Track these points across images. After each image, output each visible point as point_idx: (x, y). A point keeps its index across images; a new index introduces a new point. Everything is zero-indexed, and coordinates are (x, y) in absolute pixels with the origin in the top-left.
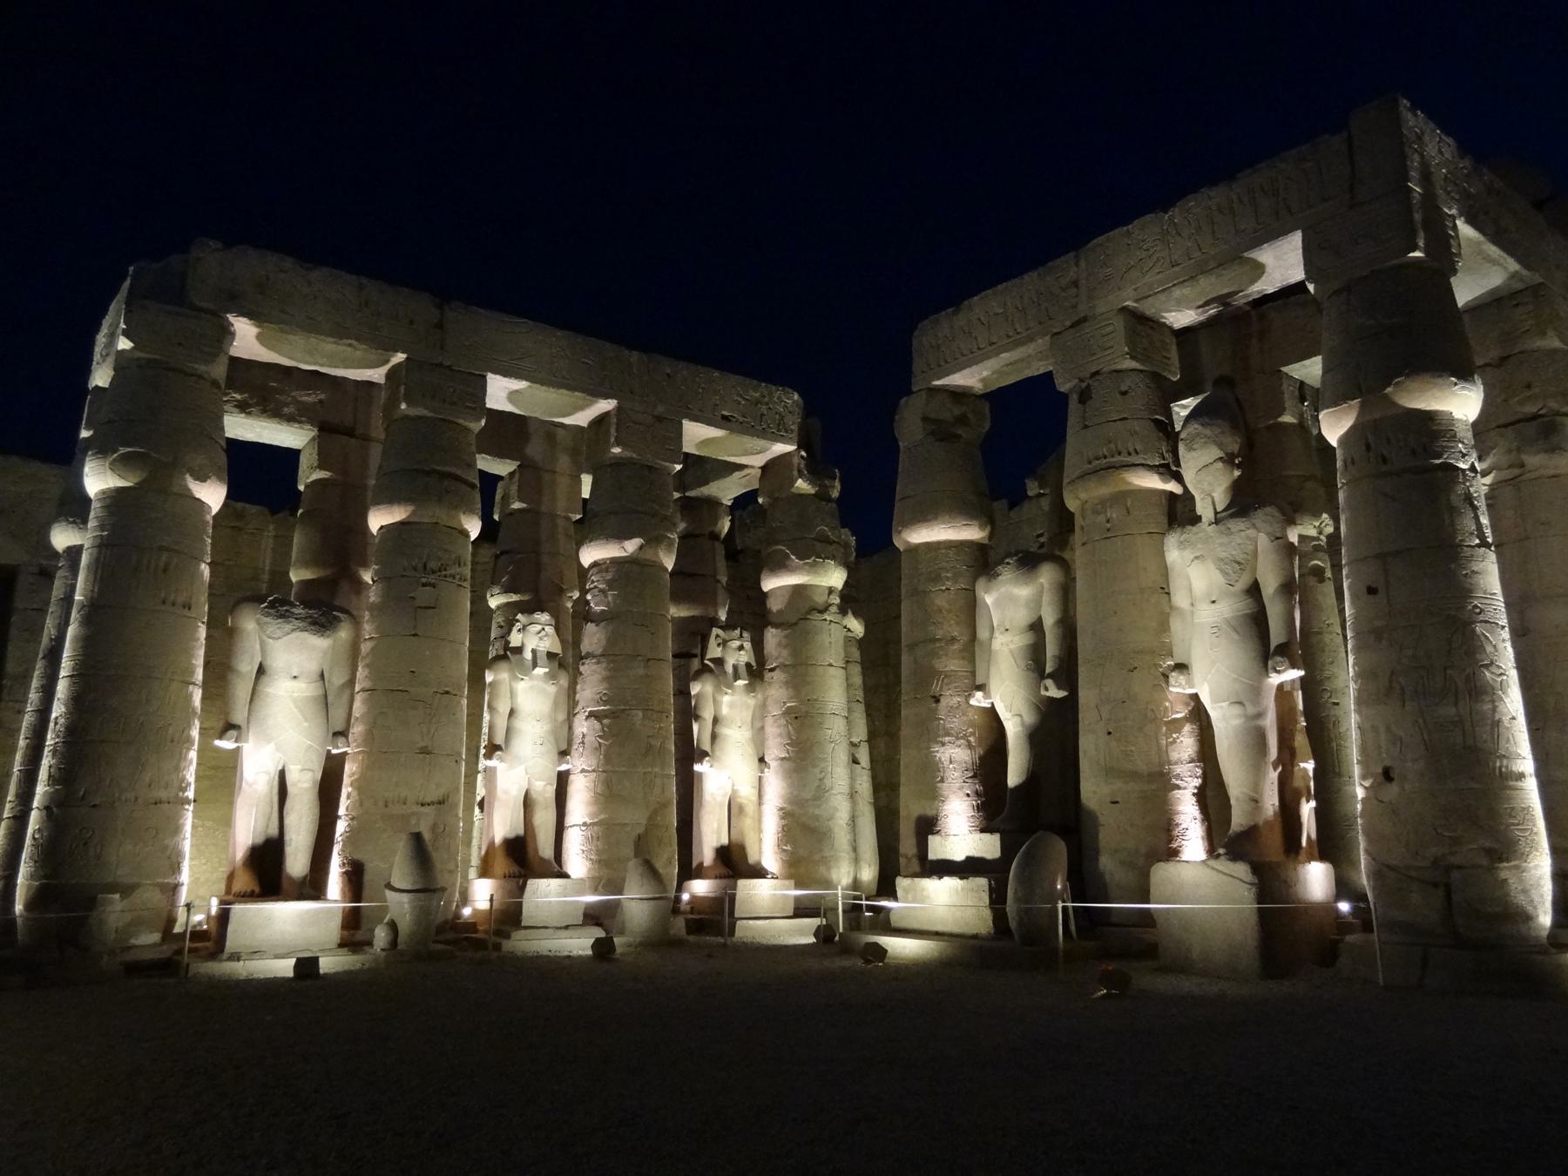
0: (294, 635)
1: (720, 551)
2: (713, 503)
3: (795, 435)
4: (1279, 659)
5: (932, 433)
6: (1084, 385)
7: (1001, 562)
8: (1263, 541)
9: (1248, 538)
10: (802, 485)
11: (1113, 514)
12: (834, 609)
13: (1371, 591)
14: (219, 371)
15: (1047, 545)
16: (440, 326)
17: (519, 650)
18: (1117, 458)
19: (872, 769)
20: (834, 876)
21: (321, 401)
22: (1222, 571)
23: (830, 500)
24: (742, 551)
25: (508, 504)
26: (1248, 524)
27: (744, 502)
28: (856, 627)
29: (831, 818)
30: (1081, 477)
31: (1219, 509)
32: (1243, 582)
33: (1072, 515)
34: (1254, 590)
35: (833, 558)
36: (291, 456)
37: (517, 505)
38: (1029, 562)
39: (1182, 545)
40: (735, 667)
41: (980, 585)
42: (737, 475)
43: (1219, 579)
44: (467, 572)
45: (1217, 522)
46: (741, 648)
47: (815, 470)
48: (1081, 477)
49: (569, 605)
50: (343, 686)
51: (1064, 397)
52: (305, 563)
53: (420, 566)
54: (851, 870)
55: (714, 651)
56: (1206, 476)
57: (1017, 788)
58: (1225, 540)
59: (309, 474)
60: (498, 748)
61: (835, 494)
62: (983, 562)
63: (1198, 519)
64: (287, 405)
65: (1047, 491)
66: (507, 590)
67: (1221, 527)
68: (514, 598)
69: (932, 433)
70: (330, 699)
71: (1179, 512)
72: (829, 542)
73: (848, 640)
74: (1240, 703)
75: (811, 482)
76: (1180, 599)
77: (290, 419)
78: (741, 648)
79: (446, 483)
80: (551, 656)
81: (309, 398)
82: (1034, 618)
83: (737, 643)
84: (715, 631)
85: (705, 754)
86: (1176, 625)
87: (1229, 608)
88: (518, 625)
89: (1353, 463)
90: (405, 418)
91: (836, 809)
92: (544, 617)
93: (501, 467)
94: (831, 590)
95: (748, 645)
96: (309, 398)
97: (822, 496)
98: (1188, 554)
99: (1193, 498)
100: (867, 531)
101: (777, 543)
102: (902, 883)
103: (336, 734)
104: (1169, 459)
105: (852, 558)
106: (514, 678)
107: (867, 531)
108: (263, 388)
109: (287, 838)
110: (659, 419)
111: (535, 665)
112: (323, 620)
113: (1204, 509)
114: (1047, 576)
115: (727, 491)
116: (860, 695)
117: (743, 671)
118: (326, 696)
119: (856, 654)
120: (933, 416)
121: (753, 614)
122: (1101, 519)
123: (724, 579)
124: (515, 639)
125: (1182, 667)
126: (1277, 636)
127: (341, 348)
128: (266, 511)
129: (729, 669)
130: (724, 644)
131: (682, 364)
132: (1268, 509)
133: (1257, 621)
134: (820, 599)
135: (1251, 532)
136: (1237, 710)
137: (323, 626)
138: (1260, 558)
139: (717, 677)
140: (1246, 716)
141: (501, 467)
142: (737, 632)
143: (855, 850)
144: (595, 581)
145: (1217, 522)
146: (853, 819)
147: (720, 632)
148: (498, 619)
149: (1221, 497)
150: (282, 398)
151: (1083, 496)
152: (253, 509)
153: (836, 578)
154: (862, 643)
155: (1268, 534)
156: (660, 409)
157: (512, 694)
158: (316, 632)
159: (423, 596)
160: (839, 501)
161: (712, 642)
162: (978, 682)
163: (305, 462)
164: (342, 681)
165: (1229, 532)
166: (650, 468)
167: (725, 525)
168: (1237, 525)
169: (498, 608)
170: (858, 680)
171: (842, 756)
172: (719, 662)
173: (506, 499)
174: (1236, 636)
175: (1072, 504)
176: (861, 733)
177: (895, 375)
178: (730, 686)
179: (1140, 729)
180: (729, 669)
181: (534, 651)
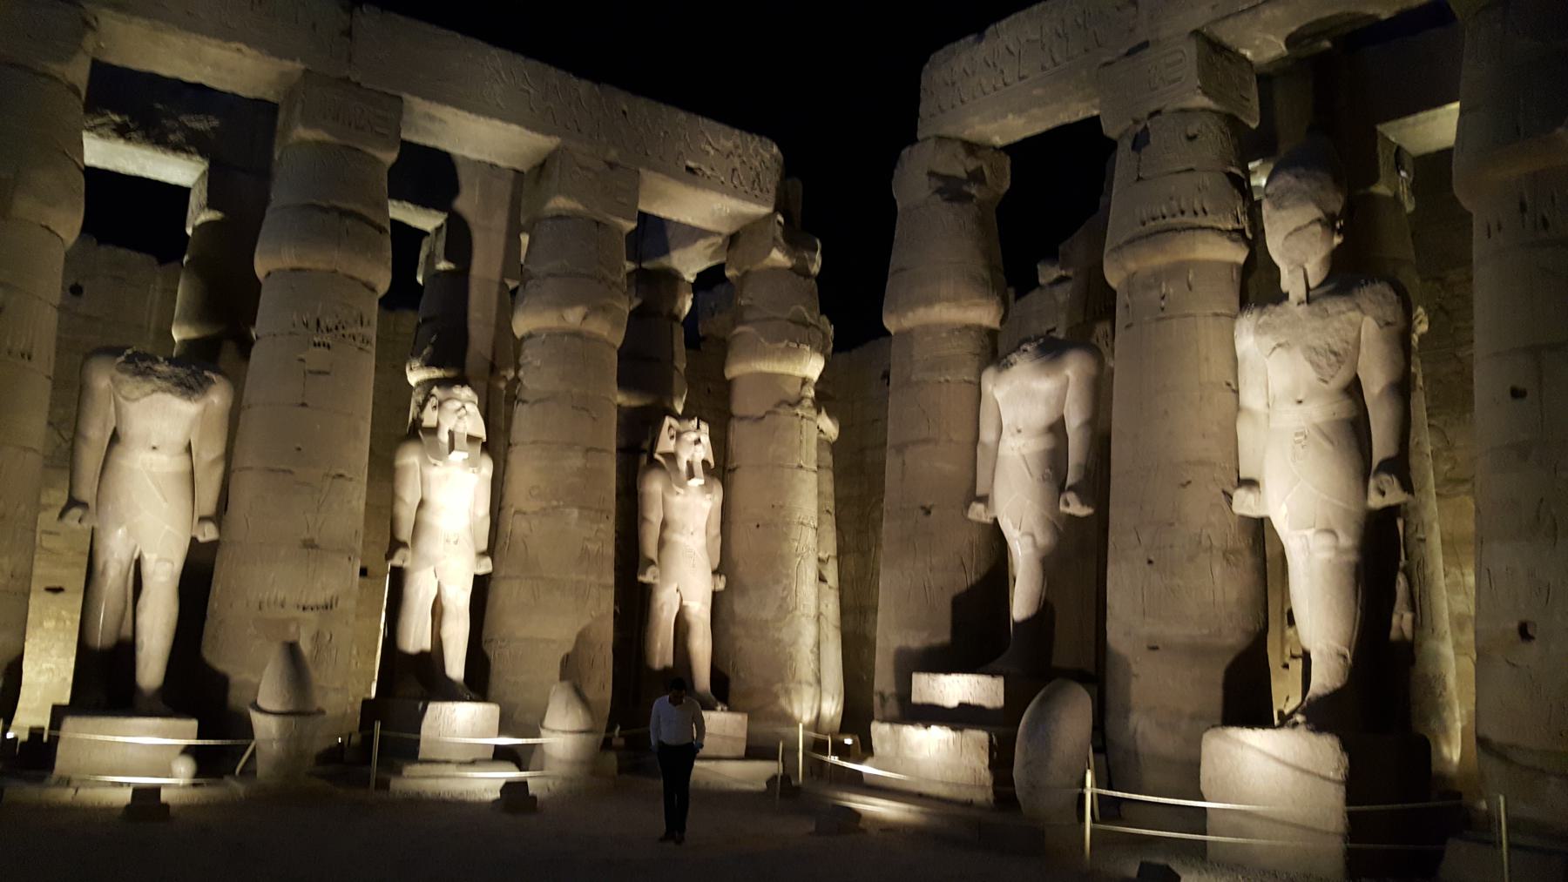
0: (155, 396)
1: (679, 335)
2: (673, 277)
3: (772, 197)
4: (1385, 477)
5: (939, 191)
6: (1140, 128)
7: (1016, 349)
8: (1369, 327)
9: (1351, 323)
10: (778, 257)
11: (1169, 289)
12: (808, 403)
13: (1517, 393)
14: (78, 73)
15: (1090, 325)
16: (348, 33)
17: (434, 431)
18: (1180, 219)
19: (841, 589)
20: (797, 713)
21: (213, 128)
22: (1312, 363)
23: (807, 275)
24: (704, 339)
25: (433, 265)
26: (1350, 305)
27: (710, 279)
28: (830, 427)
29: (794, 643)
30: (1130, 242)
31: (1312, 284)
32: (1342, 377)
33: (1113, 293)
34: (1354, 389)
35: (810, 343)
36: (182, 193)
37: (443, 265)
38: (1051, 350)
39: (1260, 330)
40: (690, 465)
41: (988, 378)
42: (701, 244)
43: (1309, 373)
44: (372, 332)
45: (1309, 300)
46: (698, 441)
47: (794, 239)
48: (1130, 242)
49: (502, 385)
50: (214, 462)
51: (1112, 145)
52: (188, 319)
53: (313, 324)
54: (815, 703)
55: (666, 444)
56: (1297, 246)
57: (1026, 622)
58: (1318, 323)
59: (199, 216)
60: (404, 545)
61: (815, 269)
62: (994, 351)
63: (1286, 296)
64: (174, 132)
65: (1070, 273)
66: (429, 364)
67: (1315, 308)
68: (437, 373)
69: (939, 191)
70: (197, 476)
71: (1257, 286)
72: (807, 325)
73: (821, 443)
74: (1331, 532)
75: (788, 253)
76: (1251, 397)
77: (177, 148)
78: (698, 441)
79: (348, 222)
80: (471, 439)
81: (200, 124)
82: (1056, 416)
83: (694, 436)
84: (668, 421)
85: (652, 562)
86: (1245, 431)
87: (1320, 411)
88: (433, 401)
89: (1500, 228)
90: (302, 143)
91: (799, 633)
92: (466, 393)
93: (427, 221)
94: (805, 381)
95: (705, 439)
96: (200, 124)
97: (800, 271)
98: (1269, 341)
99: (1275, 270)
100: (852, 311)
101: (744, 323)
102: (879, 730)
103: (202, 519)
104: (1245, 223)
105: (830, 349)
106: (425, 462)
107: (852, 311)
108: (143, 106)
109: (139, 641)
110: (611, 165)
111: (452, 448)
112: (192, 381)
113: (1291, 283)
114: (1074, 368)
115: (690, 263)
116: (830, 505)
117: (698, 468)
118: (192, 472)
119: (828, 458)
120: (942, 170)
121: (715, 405)
122: (1155, 294)
123: (681, 364)
124: (430, 418)
125: (1251, 483)
126: (1382, 446)
127: (228, 54)
128: (154, 260)
129: (683, 467)
130: (678, 436)
131: (642, 101)
132: (1378, 286)
133: (1356, 429)
134: (792, 391)
135: (1354, 315)
136: (1326, 540)
137: (190, 388)
138: (1363, 350)
139: (668, 474)
140: (1336, 548)
141: (427, 221)
142: (694, 423)
143: (819, 681)
144: (529, 355)
145: (1309, 300)
146: (818, 645)
147: (674, 422)
148: (417, 397)
149: (1315, 270)
150: (168, 123)
151: (1132, 266)
152: (137, 257)
153: (813, 367)
154: (836, 448)
155: (1376, 319)
156: (613, 154)
157: (423, 482)
158: (182, 395)
159: (316, 358)
160: (819, 278)
161: (665, 434)
162: (980, 491)
163: (194, 201)
164: (212, 456)
165: (1325, 314)
166: (598, 223)
167: (687, 304)
168: (1336, 305)
169: (418, 384)
170: (829, 488)
171: (809, 573)
172: (672, 457)
173: (431, 258)
174: (1327, 446)
175: (1113, 278)
176: (830, 548)
177: (899, 124)
178: (682, 485)
179: (1191, 559)
180: (683, 467)
181: (451, 433)
